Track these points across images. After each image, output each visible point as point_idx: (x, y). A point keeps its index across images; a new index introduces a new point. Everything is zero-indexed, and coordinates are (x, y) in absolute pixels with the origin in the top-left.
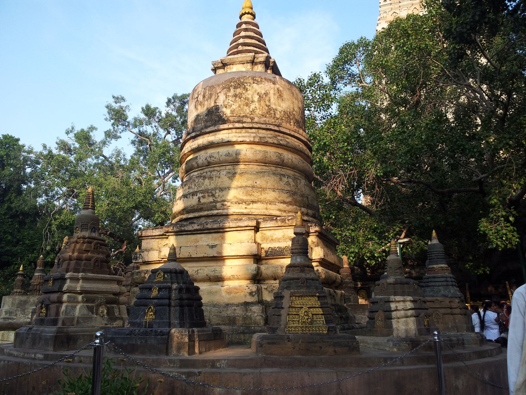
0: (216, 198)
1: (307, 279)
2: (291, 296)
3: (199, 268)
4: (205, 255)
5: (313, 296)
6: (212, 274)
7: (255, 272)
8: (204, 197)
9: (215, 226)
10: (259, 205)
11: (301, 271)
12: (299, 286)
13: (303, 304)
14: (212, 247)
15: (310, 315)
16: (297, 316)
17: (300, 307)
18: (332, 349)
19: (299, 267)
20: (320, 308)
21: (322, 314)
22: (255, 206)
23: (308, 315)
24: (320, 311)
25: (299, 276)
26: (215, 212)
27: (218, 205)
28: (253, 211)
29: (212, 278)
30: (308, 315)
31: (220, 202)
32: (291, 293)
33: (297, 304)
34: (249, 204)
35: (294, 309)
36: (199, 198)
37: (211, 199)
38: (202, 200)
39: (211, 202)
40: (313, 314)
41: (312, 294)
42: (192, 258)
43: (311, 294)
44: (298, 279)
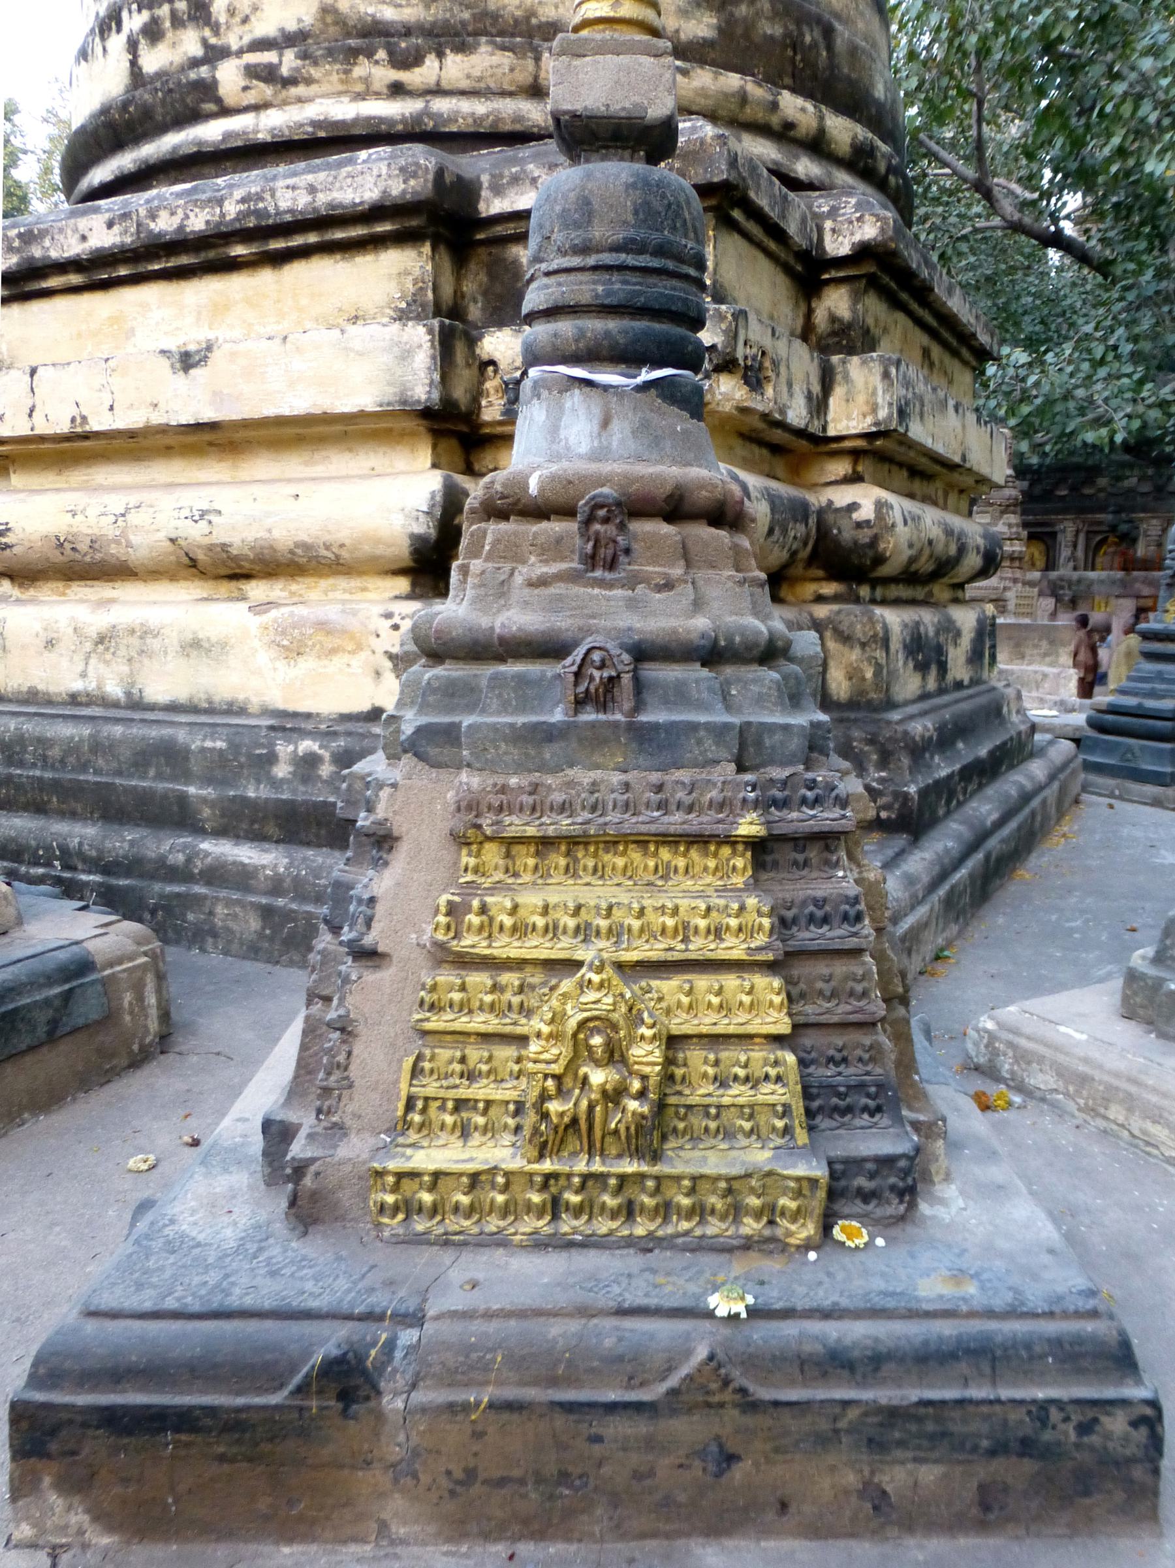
0: (216, 29)
1: (643, 653)
2: (461, 841)
3: (133, 499)
4: (157, 419)
5: (699, 840)
6: (195, 533)
7: (424, 527)
8: (153, 33)
9: (198, 222)
10: (485, 61)
11: (591, 561)
12: (548, 734)
13: (585, 932)
14: (187, 361)
15: (646, 1055)
16: (505, 1053)
17: (550, 965)
18: (851, 1479)
19: (568, 512)
20: (771, 967)
21: (777, 1040)
22: (455, 68)
23: (614, 1055)
24: (764, 1006)
25: (563, 623)
26: (211, 132)
27: (229, 77)
28: (442, 105)
29: (200, 556)
30: (614, 1055)
31: (240, 52)
32: (471, 806)
33: (520, 930)
34: (411, 61)
35: (479, 979)
36: (132, 46)
37: (190, 43)
38: (153, 60)
39: (195, 63)
40: (673, 1042)
41: (696, 823)
42: (97, 435)
43: (675, 821)
44: (549, 648)
